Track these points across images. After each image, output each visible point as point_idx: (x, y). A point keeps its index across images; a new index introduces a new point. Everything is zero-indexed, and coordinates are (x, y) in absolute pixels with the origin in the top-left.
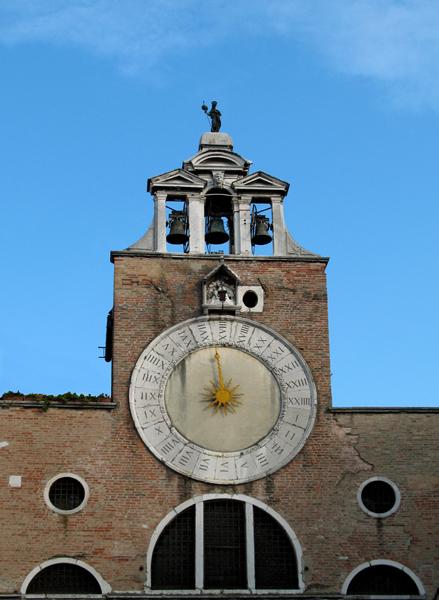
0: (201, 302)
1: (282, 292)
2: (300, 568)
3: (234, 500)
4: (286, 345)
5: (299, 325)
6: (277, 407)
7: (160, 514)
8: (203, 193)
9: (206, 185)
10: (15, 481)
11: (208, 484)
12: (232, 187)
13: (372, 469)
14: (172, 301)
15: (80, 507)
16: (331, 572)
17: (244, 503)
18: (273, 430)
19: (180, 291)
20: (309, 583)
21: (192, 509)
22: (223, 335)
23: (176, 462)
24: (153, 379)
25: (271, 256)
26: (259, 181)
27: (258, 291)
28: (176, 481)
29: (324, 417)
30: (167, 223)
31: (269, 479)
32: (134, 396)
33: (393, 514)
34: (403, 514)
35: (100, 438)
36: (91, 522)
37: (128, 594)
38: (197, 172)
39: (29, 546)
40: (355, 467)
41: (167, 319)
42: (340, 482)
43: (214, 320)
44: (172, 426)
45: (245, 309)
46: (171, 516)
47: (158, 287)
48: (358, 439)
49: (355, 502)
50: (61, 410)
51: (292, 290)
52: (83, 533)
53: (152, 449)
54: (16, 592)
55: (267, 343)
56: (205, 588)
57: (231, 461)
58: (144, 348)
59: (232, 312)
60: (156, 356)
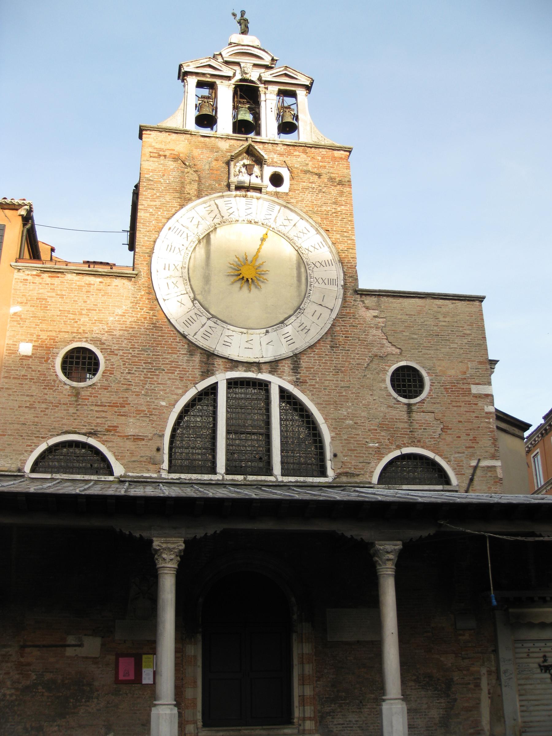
0: (229, 178)
1: (308, 175)
2: (328, 455)
3: (259, 379)
4: (312, 226)
5: (324, 208)
6: (303, 286)
7: (180, 391)
11: (232, 361)
12: (260, 79)
13: (401, 353)
14: (199, 177)
16: (361, 460)
17: (270, 382)
18: (298, 309)
19: (207, 167)
20: (339, 471)
22: (249, 211)
23: (198, 336)
25: (297, 141)
28: (197, 358)
29: (351, 298)
30: (196, 105)
33: (422, 402)
34: (432, 401)
35: (119, 307)
36: (105, 397)
37: (142, 477)
38: (227, 63)
39: (36, 420)
40: (384, 350)
41: (193, 192)
42: (368, 365)
46: (192, 393)
48: (386, 322)
50: (80, 277)
51: (316, 174)
52: (97, 408)
54: (19, 470)
55: (293, 223)
56: (227, 474)
58: (169, 219)
59: (259, 190)
60: (181, 228)
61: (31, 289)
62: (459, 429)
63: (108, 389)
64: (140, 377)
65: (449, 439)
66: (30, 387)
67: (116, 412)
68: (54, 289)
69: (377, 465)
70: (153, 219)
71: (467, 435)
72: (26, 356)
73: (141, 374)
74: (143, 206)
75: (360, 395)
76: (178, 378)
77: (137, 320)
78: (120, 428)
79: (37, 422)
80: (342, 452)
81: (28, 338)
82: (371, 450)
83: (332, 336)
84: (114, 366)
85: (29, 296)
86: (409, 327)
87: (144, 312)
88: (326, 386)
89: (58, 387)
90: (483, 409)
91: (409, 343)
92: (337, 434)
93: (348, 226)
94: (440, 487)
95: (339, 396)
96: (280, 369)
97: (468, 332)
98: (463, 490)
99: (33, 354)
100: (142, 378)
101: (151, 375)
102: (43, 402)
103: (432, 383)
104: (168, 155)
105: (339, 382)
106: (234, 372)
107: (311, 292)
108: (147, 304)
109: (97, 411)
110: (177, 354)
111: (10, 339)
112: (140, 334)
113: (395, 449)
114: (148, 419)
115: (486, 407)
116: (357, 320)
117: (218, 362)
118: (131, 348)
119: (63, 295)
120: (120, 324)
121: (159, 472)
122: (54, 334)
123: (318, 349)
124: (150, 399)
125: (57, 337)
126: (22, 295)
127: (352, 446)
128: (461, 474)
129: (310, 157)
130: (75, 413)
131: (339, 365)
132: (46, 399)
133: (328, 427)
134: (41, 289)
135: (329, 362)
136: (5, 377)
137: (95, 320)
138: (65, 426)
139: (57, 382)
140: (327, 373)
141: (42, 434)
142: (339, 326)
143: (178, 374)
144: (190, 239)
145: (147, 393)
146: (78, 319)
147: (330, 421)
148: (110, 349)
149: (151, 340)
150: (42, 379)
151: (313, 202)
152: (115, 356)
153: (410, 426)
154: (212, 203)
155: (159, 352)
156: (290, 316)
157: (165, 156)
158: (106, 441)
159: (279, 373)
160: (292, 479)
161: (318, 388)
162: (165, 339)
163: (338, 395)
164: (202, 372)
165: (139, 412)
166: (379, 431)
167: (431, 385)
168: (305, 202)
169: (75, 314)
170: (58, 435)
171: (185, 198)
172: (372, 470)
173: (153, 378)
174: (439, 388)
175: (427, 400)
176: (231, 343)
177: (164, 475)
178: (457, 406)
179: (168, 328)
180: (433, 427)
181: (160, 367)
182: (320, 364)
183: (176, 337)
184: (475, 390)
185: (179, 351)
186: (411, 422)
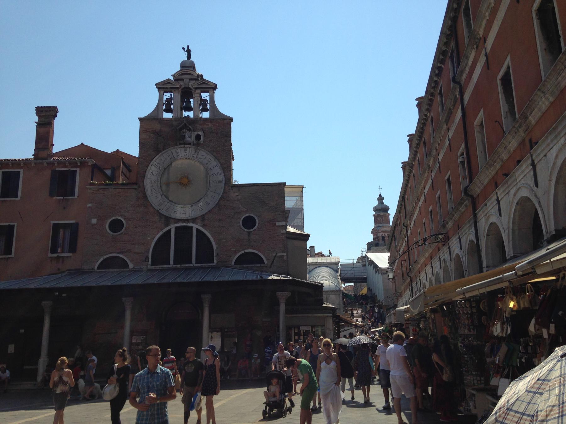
2: (215, 254)
7: (156, 233)
8: (179, 90)
9: (181, 86)
10: (94, 221)
13: (247, 211)
15: (122, 231)
21: (170, 230)
22: (186, 154)
24: (155, 174)
26: (204, 83)
27: (200, 133)
28: (163, 219)
31: (203, 217)
44: (163, 195)
46: (161, 233)
47: (157, 133)
49: (239, 225)
54: (92, 269)
55: (204, 157)
58: (151, 161)
71: (272, 243)
72: (94, 224)
90: (281, 232)
94: (259, 265)
97: (276, 199)
109: (123, 244)
113: (242, 251)
115: (282, 231)
121: (147, 266)
133: (215, 243)
144: (160, 168)
156: (202, 198)
157: (150, 132)
160: (199, 265)
172: (232, 259)
176: (177, 212)
186: (250, 239)
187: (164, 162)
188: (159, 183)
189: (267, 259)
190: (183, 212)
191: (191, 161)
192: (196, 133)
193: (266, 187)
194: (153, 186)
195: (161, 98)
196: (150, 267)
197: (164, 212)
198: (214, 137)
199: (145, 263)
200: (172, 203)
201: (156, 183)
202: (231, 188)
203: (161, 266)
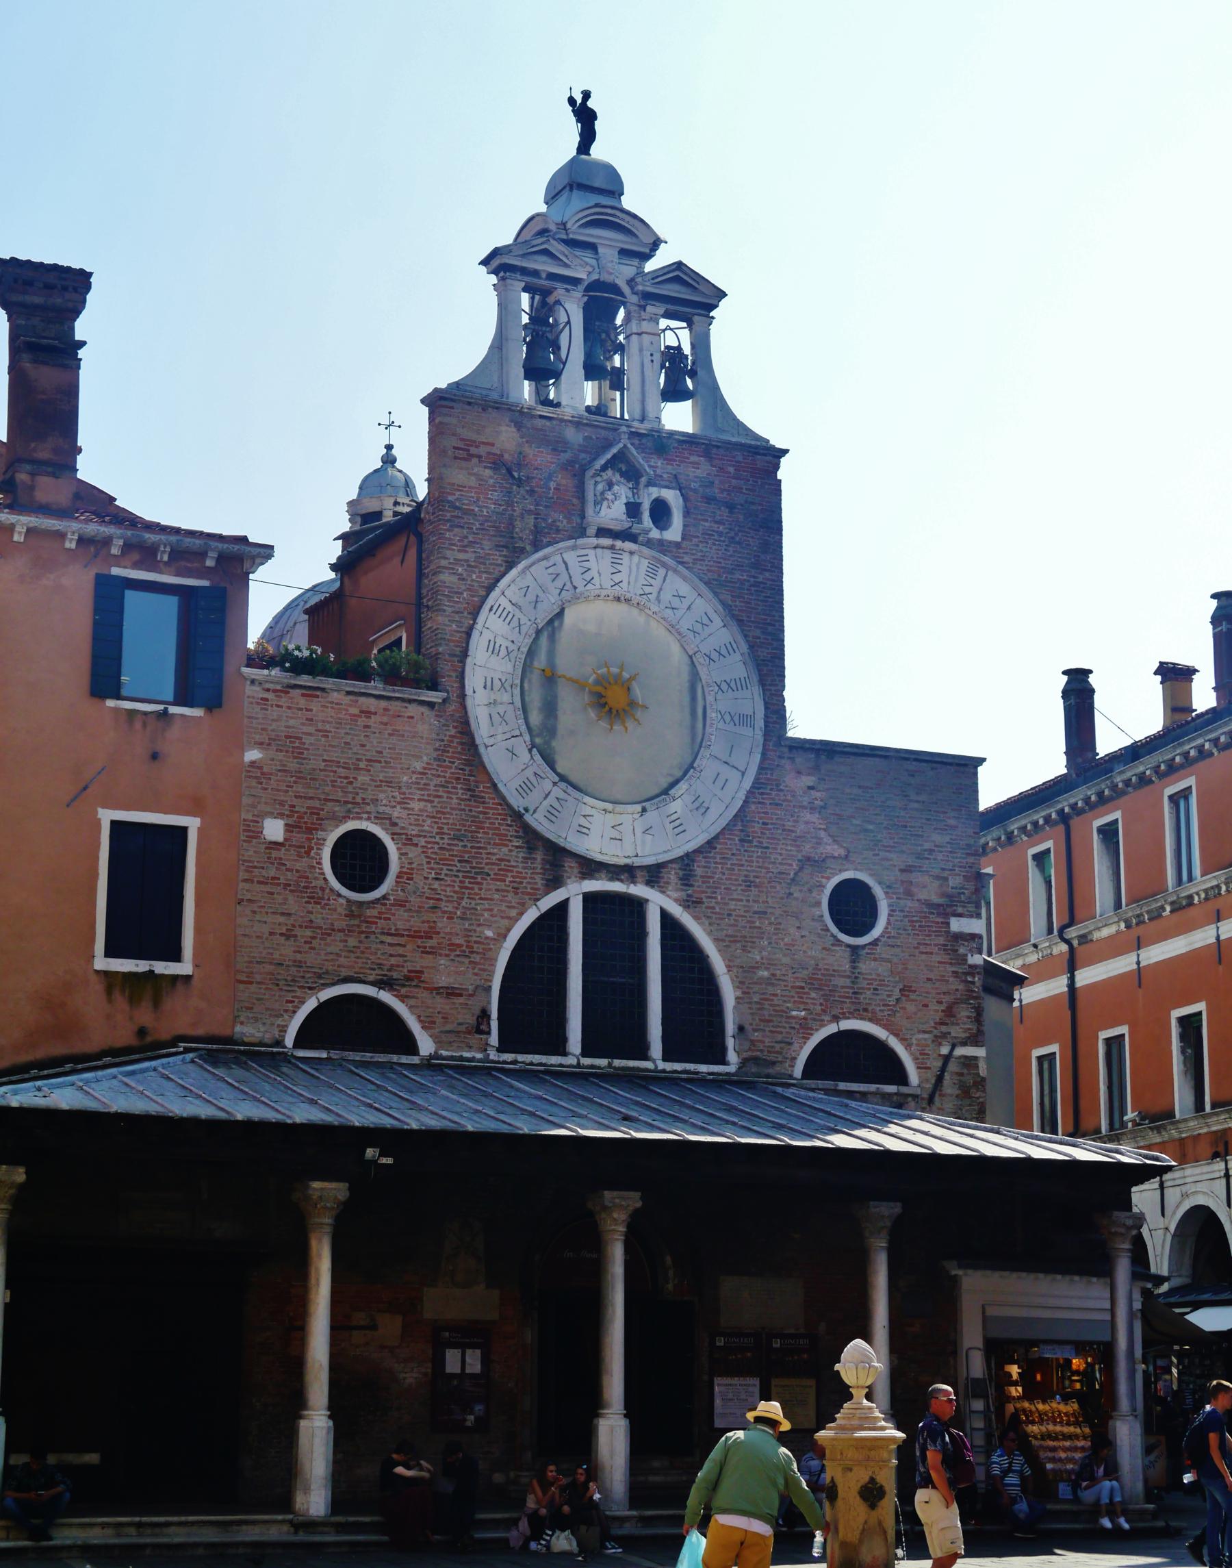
2: (730, 1027)
3: (630, 895)
7: (513, 913)
8: (581, 287)
10: (274, 829)
16: (779, 1037)
17: (647, 901)
20: (745, 1055)
21: (563, 907)
22: (617, 578)
23: (539, 815)
24: (503, 652)
27: (671, 496)
28: (539, 856)
31: (686, 861)
32: (474, 681)
33: (875, 943)
34: (891, 941)
35: (418, 757)
36: (401, 919)
37: (462, 1059)
38: (573, 243)
39: (299, 957)
40: (821, 849)
41: (527, 535)
42: (796, 874)
43: (603, 548)
45: (655, 534)
46: (531, 915)
52: (389, 939)
53: (500, 786)
55: (686, 603)
56: (585, 1053)
57: (627, 820)
58: (490, 589)
60: (509, 607)
61: (275, 717)
62: (927, 993)
63: (405, 906)
64: (454, 886)
65: (911, 1008)
66: (286, 899)
67: (418, 947)
68: (311, 720)
69: (801, 1048)
70: (463, 587)
71: (938, 1002)
72: (276, 843)
73: (454, 881)
74: (447, 561)
75: (781, 927)
76: (510, 889)
77: (446, 782)
78: (426, 975)
79: (300, 962)
80: (751, 1024)
81: (275, 809)
82: (794, 1021)
83: (742, 821)
84: (413, 866)
85: (273, 730)
86: (862, 809)
87: (456, 768)
88: (730, 910)
89: (329, 899)
90: (966, 960)
91: (860, 839)
92: (744, 993)
93: (774, 613)
94: (891, 1089)
95: (750, 927)
96: (663, 878)
97: (952, 822)
98: (925, 1096)
99: (286, 840)
100: (457, 889)
101: (470, 883)
102: (306, 927)
103: (892, 911)
104: (483, 454)
105: (751, 904)
106: (594, 882)
107: (713, 737)
108: (459, 753)
109: (390, 945)
110: (507, 846)
111: (248, 811)
112: (452, 809)
113: (831, 1022)
114: (467, 961)
115: (969, 955)
116: (782, 794)
117: (570, 865)
118: (437, 833)
119: (327, 731)
120: (419, 789)
121: (486, 1050)
122: (316, 804)
123: (721, 844)
124: (470, 925)
125: (323, 810)
126: (262, 729)
127: (766, 1013)
128: (925, 1068)
129: (715, 466)
130: (359, 947)
131: (752, 874)
132: (311, 921)
134: (292, 718)
135: (736, 868)
136: (245, 881)
137: (381, 781)
138: (343, 970)
139: (327, 891)
140: (733, 888)
141: (307, 982)
142: (754, 803)
143: (510, 882)
144: (524, 629)
145: (464, 913)
146: (354, 778)
147: (735, 970)
148: (406, 834)
149: (468, 821)
150: (303, 885)
151: (720, 563)
152: (413, 848)
153: (853, 982)
154: (558, 558)
155: (480, 842)
156: (677, 782)
157: (479, 457)
158: (407, 997)
159: (662, 884)
160: (678, 1066)
161: (719, 913)
162: (489, 818)
163: (748, 925)
164: (547, 880)
165: (453, 946)
166: (807, 990)
167: (889, 915)
168: (706, 563)
169: (349, 769)
170: (334, 984)
171: (515, 547)
172: (794, 1054)
173: (472, 889)
174: (901, 921)
175: (883, 939)
177: (493, 1055)
178: (926, 953)
179: (493, 799)
180: (888, 986)
181: (483, 868)
182: (724, 871)
183: (506, 815)
184: (956, 925)
185: (510, 841)
186: (856, 978)
187: (536, 602)
188: (519, 688)
189: (920, 1067)
190: (615, 834)
191: (635, 611)
192: (655, 492)
193: (912, 766)
194: (495, 702)
195: (506, 310)
196: (496, 1059)
197: (539, 822)
198: (720, 523)
199: (477, 1036)
200: (570, 789)
201: (509, 688)
202: (786, 750)
203: (537, 1058)
